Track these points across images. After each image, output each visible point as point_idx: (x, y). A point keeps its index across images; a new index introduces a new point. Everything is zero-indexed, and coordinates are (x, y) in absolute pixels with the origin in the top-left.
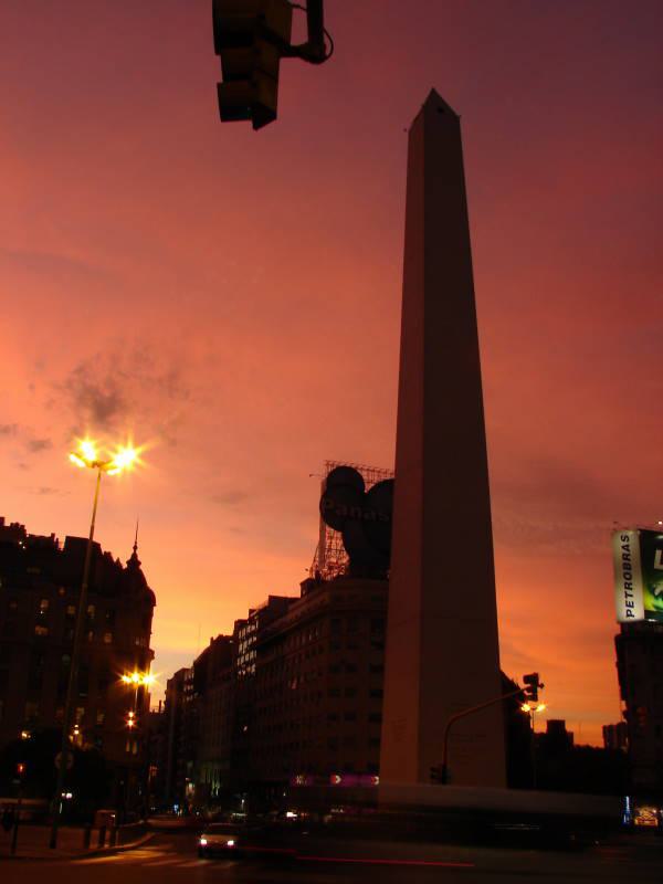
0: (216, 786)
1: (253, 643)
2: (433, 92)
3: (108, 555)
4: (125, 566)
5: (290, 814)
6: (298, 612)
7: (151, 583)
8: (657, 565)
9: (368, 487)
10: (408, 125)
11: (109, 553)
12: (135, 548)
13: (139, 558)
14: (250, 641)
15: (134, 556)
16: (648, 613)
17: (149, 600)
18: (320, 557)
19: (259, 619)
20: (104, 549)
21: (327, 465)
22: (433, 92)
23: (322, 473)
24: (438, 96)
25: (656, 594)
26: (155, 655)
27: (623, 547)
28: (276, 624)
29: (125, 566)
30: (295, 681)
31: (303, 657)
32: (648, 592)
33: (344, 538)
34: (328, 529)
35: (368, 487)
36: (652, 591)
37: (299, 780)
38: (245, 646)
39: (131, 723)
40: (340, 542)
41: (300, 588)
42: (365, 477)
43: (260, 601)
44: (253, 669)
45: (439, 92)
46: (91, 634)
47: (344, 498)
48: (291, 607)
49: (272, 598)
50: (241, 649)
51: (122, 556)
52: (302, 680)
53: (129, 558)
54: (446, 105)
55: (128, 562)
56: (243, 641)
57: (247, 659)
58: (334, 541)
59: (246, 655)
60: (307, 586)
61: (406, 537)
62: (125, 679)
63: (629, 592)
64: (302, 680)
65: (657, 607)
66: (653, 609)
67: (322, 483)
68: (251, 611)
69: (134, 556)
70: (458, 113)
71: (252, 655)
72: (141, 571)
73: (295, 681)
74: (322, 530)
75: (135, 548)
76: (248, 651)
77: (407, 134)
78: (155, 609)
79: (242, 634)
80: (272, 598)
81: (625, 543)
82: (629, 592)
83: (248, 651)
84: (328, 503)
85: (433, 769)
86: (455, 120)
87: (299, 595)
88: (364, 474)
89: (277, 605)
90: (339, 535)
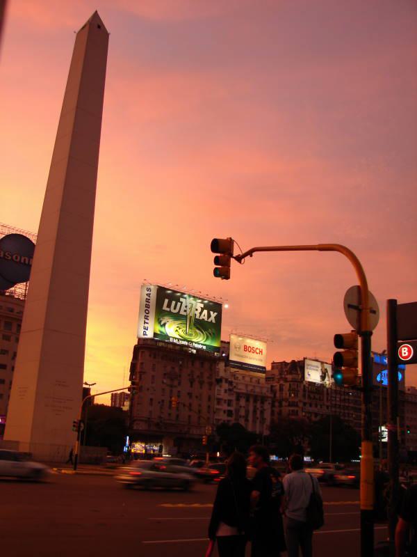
2: (96, 15)
8: (165, 308)
10: (78, 29)
16: (155, 334)
22: (96, 15)
24: (98, 15)
25: (162, 323)
27: (147, 294)
32: (157, 323)
36: (160, 322)
45: (99, 13)
54: (102, 23)
63: (146, 321)
65: (161, 332)
70: (109, 32)
77: (75, 35)
81: (149, 292)
82: (146, 321)
86: (106, 35)
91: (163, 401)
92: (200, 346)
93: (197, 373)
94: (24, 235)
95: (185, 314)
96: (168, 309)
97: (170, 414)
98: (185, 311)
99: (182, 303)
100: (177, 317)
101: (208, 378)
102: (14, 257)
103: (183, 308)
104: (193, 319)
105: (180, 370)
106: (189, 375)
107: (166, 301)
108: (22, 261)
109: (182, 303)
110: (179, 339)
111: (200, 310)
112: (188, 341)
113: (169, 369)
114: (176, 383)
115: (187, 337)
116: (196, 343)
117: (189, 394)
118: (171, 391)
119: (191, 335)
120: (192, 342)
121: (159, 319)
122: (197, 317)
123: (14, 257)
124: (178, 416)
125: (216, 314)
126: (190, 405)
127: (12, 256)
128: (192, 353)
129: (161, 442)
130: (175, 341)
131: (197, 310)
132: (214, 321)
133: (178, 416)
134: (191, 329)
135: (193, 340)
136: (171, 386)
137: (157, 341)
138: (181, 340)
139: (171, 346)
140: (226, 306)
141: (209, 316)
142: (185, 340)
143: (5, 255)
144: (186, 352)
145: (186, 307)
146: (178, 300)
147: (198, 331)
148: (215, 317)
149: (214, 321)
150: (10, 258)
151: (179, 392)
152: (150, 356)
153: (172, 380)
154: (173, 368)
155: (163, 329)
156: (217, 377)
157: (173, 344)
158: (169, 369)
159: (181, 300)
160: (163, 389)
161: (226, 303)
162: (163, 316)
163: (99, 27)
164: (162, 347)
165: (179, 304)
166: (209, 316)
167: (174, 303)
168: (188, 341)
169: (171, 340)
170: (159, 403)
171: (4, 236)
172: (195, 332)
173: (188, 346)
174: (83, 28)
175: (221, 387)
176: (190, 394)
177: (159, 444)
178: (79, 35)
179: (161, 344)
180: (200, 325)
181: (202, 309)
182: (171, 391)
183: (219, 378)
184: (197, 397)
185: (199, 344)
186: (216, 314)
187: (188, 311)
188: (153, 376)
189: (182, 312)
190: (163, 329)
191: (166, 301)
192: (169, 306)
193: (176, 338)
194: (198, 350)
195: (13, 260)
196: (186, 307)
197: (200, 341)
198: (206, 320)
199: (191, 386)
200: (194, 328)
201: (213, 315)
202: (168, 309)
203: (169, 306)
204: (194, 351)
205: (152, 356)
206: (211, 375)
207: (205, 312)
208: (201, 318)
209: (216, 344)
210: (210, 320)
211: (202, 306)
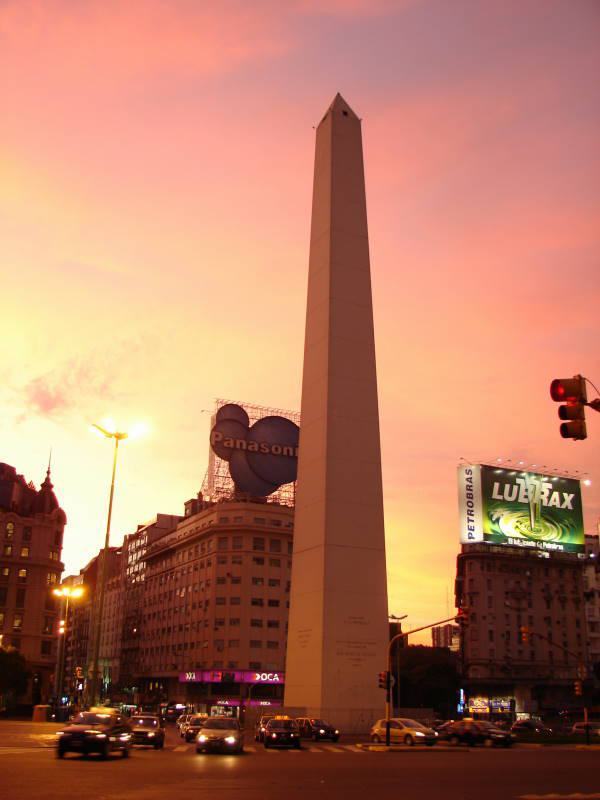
0: (107, 681)
1: (146, 555)
2: (339, 99)
3: (21, 477)
4: (38, 488)
5: (179, 706)
6: (187, 530)
7: (63, 504)
8: (495, 495)
9: (252, 423)
10: (317, 123)
11: (22, 476)
12: (48, 473)
13: (52, 482)
14: (140, 553)
15: (48, 480)
16: (486, 536)
17: (60, 519)
18: (209, 482)
19: (147, 534)
20: (18, 472)
21: (217, 402)
22: (339, 99)
23: (213, 409)
26: (65, 568)
27: (467, 479)
28: (167, 539)
29: (38, 488)
30: (184, 590)
31: (191, 570)
33: (232, 469)
34: (217, 459)
35: (252, 423)
36: (490, 517)
37: (190, 676)
38: (135, 558)
39: (62, 631)
40: (227, 471)
41: (183, 507)
42: (249, 415)
43: (149, 519)
44: (143, 576)
45: (342, 95)
46: (9, 549)
47: (233, 431)
48: (180, 525)
49: (160, 516)
50: (130, 560)
51: (36, 481)
52: (190, 589)
53: (43, 481)
54: (350, 109)
55: (42, 485)
56: (132, 553)
57: (136, 569)
58: (221, 469)
59: (135, 565)
60: (195, 506)
61: (291, 474)
62: (57, 593)
63: (471, 518)
64: (190, 589)
65: (493, 531)
66: (491, 533)
67: (212, 419)
68: (140, 527)
69: (48, 480)
70: (359, 117)
71: (142, 565)
72: (52, 495)
73: (184, 590)
74: (211, 460)
75: (48, 473)
76: (137, 562)
78: (66, 528)
79: (132, 546)
80: (160, 516)
81: (469, 476)
82: (471, 518)
83: (137, 562)
84: (217, 436)
85: (380, 675)
86: (357, 123)
87: (182, 514)
88: (249, 411)
89: (165, 524)
90: (226, 463)
91: (508, 633)
92: (554, 547)
93: (555, 586)
94: (283, 416)
95: (526, 501)
96: (500, 497)
97: (520, 652)
98: (526, 497)
99: (519, 485)
100: (515, 506)
101: (573, 592)
102: (273, 449)
103: (522, 493)
104: (539, 507)
105: (529, 584)
106: (543, 591)
107: (497, 485)
108: (285, 453)
109: (519, 485)
110: (521, 540)
111: (547, 493)
112: (536, 541)
113: (512, 584)
114: (524, 604)
115: (532, 534)
116: (547, 542)
117: (545, 619)
118: (519, 617)
119: (539, 531)
120: (542, 541)
121: (488, 513)
122: (545, 504)
123: (273, 449)
124: (533, 654)
125: (572, 496)
126: (550, 635)
127: (270, 449)
128: (543, 558)
129: (513, 696)
130: (517, 543)
131: (543, 493)
132: (570, 507)
133: (533, 654)
134: (538, 522)
135: (543, 539)
136: (518, 610)
137: (489, 545)
138: (526, 540)
139: (511, 551)
140: (586, 483)
141: (562, 500)
142: (530, 539)
143: (260, 448)
144: (535, 557)
145: (526, 490)
146: (512, 482)
147: (548, 524)
148: (573, 501)
149: (570, 507)
150: (267, 451)
151: (531, 617)
152: (482, 568)
153: (518, 600)
154: (518, 582)
155: (495, 527)
156: (585, 590)
157: (515, 547)
158: (512, 584)
159: (518, 481)
160: (507, 616)
161: (586, 479)
162: (497, 507)
163: (345, 113)
164: (498, 553)
165: (515, 488)
166: (562, 500)
167: (507, 487)
168: (536, 541)
169: (510, 542)
170: (503, 635)
171: (255, 421)
172: (545, 526)
173: (537, 549)
174: (324, 119)
175: (593, 604)
176: (547, 619)
177: (509, 698)
178: (320, 129)
179: (496, 549)
180: (550, 515)
181: (551, 492)
182: (519, 617)
183: (588, 591)
184: (558, 622)
185: (552, 543)
186: (572, 496)
187: (530, 496)
188: (490, 598)
189: (522, 500)
190: (495, 527)
191: (497, 485)
192: (501, 492)
193: (517, 539)
194: (552, 552)
195: (271, 452)
196: (526, 490)
197: (553, 539)
198: (558, 506)
199: (548, 607)
200: (542, 521)
201: (568, 498)
202: (500, 497)
203: (501, 492)
204: (547, 555)
205: (485, 568)
206: (576, 587)
207: (556, 495)
208: (550, 505)
209: (578, 541)
210: (564, 507)
211: (550, 486)
